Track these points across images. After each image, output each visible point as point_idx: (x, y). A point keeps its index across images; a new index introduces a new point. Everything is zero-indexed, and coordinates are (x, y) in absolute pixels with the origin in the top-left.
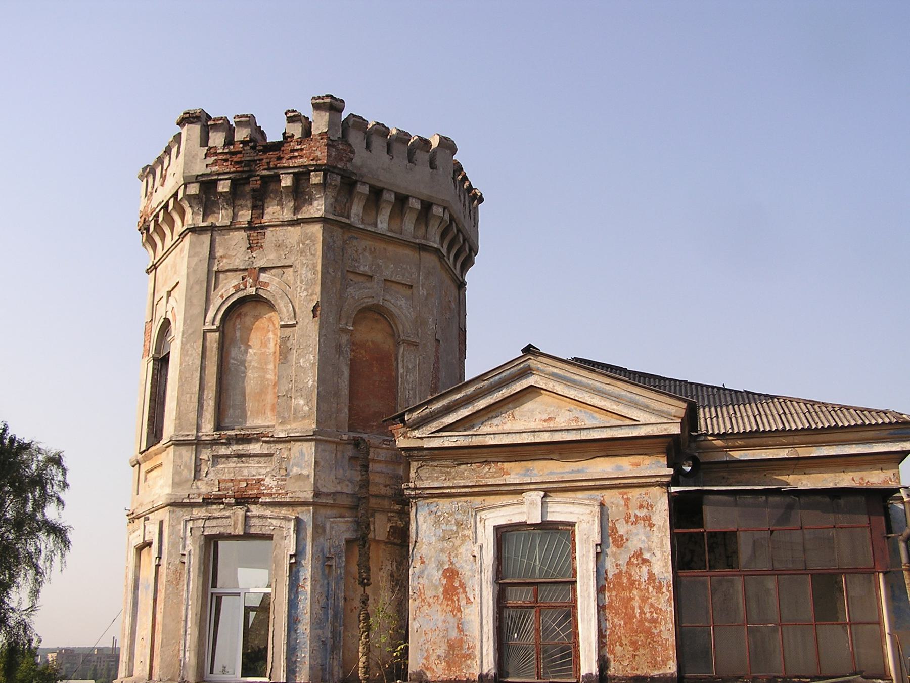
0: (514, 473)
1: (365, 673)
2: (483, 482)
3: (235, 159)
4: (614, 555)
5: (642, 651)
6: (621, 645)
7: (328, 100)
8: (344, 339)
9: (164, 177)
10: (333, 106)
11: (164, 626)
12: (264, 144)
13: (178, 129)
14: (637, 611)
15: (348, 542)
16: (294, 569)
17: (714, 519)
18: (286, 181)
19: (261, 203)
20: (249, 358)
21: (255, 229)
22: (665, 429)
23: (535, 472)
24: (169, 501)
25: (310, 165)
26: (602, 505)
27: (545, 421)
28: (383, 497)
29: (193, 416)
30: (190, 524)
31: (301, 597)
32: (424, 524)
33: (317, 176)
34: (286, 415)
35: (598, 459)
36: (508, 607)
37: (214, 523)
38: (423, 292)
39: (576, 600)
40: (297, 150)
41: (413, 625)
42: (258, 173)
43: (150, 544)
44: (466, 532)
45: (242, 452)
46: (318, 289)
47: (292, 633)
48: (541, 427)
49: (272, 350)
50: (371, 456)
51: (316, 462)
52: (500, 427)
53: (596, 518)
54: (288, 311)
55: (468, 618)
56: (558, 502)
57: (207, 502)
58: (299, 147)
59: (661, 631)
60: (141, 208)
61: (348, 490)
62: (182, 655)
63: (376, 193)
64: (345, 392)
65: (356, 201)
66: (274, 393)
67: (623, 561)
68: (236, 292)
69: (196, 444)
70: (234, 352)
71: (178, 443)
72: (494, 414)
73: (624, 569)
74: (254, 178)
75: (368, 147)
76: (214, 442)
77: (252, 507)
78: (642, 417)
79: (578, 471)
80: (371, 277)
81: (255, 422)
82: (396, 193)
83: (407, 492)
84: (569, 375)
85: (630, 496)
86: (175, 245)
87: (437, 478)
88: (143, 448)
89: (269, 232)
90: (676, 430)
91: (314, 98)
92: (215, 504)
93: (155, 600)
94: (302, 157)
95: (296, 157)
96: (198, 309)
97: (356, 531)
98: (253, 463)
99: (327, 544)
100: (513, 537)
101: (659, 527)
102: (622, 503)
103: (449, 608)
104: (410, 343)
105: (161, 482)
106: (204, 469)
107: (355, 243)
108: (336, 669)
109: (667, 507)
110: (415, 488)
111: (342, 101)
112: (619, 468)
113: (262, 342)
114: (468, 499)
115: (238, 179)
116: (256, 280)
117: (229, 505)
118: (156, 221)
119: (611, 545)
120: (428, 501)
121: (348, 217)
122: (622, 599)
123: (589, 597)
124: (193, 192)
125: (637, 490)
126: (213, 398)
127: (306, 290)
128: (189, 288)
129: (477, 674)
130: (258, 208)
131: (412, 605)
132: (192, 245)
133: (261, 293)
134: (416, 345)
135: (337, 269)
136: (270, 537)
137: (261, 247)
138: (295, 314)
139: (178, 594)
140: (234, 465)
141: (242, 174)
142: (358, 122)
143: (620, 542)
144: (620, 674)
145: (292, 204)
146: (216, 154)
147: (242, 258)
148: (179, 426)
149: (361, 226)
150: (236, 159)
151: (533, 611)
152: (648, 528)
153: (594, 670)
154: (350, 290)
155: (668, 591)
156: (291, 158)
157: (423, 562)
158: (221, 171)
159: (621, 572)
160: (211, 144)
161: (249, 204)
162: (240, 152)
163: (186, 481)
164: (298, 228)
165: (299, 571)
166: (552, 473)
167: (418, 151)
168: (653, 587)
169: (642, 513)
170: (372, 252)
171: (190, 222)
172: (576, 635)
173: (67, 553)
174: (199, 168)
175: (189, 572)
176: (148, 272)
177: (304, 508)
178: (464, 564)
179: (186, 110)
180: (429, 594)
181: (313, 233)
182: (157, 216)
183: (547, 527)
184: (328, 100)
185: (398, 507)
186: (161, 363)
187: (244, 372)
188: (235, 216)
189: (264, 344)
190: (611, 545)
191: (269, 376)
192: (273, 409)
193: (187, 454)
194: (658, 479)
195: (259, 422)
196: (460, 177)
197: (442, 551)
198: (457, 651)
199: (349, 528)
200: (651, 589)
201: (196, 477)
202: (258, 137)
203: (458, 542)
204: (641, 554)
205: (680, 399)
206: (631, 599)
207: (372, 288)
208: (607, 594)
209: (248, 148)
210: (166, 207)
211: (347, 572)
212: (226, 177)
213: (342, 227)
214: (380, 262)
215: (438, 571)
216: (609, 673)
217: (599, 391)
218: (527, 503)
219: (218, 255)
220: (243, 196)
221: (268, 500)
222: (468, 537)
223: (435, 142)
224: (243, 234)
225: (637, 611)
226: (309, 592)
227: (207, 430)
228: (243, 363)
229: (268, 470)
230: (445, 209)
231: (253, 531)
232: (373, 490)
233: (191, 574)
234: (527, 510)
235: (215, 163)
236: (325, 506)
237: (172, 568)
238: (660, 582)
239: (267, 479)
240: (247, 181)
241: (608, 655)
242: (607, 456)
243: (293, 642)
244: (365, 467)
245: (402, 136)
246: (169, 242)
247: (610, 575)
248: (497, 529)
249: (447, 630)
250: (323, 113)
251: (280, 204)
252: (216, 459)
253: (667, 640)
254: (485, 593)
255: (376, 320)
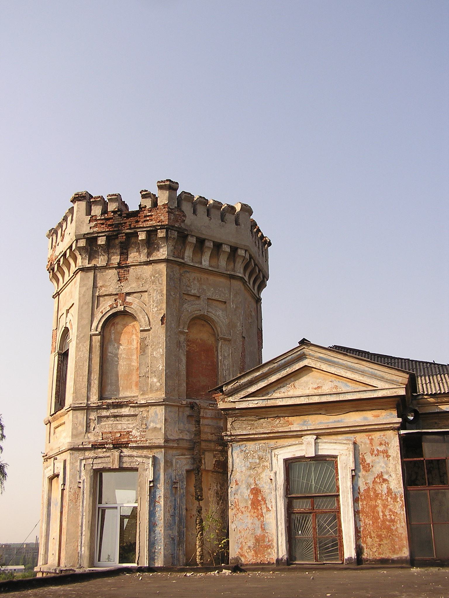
0: (296, 424)
1: (201, 559)
2: (276, 430)
3: (109, 223)
4: (364, 477)
5: (385, 541)
6: (371, 537)
7: (168, 183)
8: (182, 338)
9: (63, 236)
10: (170, 186)
11: (68, 530)
12: (127, 212)
13: (72, 205)
14: (381, 514)
15: (188, 471)
16: (152, 491)
17: (430, 451)
18: (142, 236)
19: (126, 251)
20: (120, 352)
21: (122, 268)
22: (395, 392)
23: (310, 422)
24: (70, 447)
25: (157, 225)
26: (355, 443)
27: (315, 389)
28: (210, 441)
29: (85, 391)
30: (84, 462)
31: (158, 509)
32: (238, 459)
33: (162, 232)
34: (145, 389)
35: (351, 413)
36: (294, 513)
37: (99, 461)
38: (233, 306)
39: (339, 508)
40: (148, 216)
41: (232, 527)
42: (123, 231)
43: (57, 476)
44: (266, 464)
45: (117, 414)
46: (164, 306)
47: (152, 533)
48: (313, 393)
49: (135, 347)
50: (202, 414)
51: (165, 419)
52: (286, 394)
53: (351, 453)
54: (145, 321)
55: (268, 520)
56: (325, 442)
57: (95, 447)
58: (150, 214)
59: (397, 528)
60: (49, 256)
61: (187, 437)
62: (79, 550)
63: (201, 242)
64: (184, 372)
65: (188, 248)
66: (137, 374)
67: (370, 481)
68: (111, 309)
69: (87, 409)
70: (110, 349)
71: (75, 409)
72: (281, 385)
73: (371, 486)
74: (121, 235)
75: (195, 212)
76: (99, 408)
77: (124, 450)
78: (380, 384)
79: (338, 421)
80: (199, 297)
81: (125, 394)
82: (213, 242)
83: (225, 438)
84: (330, 358)
85: (373, 437)
86: (71, 280)
87: (245, 428)
88: (53, 412)
89: (131, 269)
90: (402, 392)
91: (159, 182)
92: (100, 448)
93: (61, 513)
94: (152, 220)
95: (148, 220)
96: (87, 321)
97: (193, 464)
98: (124, 421)
99: (174, 474)
100: (296, 467)
101: (394, 457)
102: (368, 442)
103: (255, 515)
104: (225, 340)
105: (64, 434)
106: (92, 425)
107: (188, 275)
108: (181, 557)
109: (398, 444)
110: (231, 435)
111: (177, 183)
112: (365, 419)
113: (128, 341)
114: (266, 441)
115: (111, 236)
116: (124, 301)
117: (109, 449)
118: (59, 264)
119: (362, 470)
120: (240, 443)
121: (183, 259)
122: (370, 506)
123: (348, 505)
124: (82, 245)
125: (378, 433)
126: (97, 379)
127: (156, 307)
128: (80, 307)
129: (275, 558)
130: (124, 254)
131: (231, 513)
132: (82, 279)
133: (127, 309)
134: (229, 340)
135: (177, 294)
136: (136, 470)
137: (127, 279)
138: (149, 322)
139: (76, 509)
140: (111, 423)
141: (113, 232)
142: (188, 196)
143: (368, 468)
144: (371, 557)
145: (146, 251)
146: (96, 220)
147: (114, 287)
148: (75, 398)
150: (109, 223)
151: (311, 515)
152: (386, 459)
153: (353, 555)
154: (185, 306)
155: (401, 500)
156: (145, 221)
157: (237, 484)
158: (100, 231)
159: (369, 488)
160: (93, 213)
161: (118, 252)
162: (112, 218)
163: (81, 433)
164: (151, 266)
165: (155, 492)
166: (321, 423)
167: (227, 214)
168: (391, 498)
169: (381, 448)
171: (80, 264)
172: (340, 531)
173: (5, 482)
174: (86, 229)
175: (83, 494)
176: (54, 297)
177: (158, 450)
178: (264, 485)
179: (76, 192)
180: (242, 505)
181: (160, 270)
182: (59, 261)
183: (318, 459)
184: (168, 183)
185: (220, 448)
186: (63, 356)
187: (118, 362)
188: (109, 260)
189: (130, 342)
190: (362, 470)
191: (133, 364)
192: (137, 385)
193: (81, 416)
194: (392, 425)
195: (128, 394)
196: (255, 230)
197: (250, 476)
198: (261, 543)
199: (188, 463)
200: (389, 499)
201: (87, 431)
202: (123, 208)
203: (260, 470)
204: (382, 475)
205: (404, 372)
206: (376, 506)
207: (200, 304)
208: (360, 503)
209: (117, 215)
210: (65, 255)
211: (187, 492)
212: (103, 234)
213: (179, 265)
215: (247, 489)
216: (363, 556)
217: (350, 368)
218: (305, 443)
219: (99, 285)
220: (114, 247)
221: (134, 445)
222: (267, 466)
223: (238, 208)
224: (115, 271)
225: (381, 514)
226: (163, 506)
227: (94, 400)
228: (116, 355)
229: (134, 425)
230: (246, 251)
231: (125, 465)
232: (203, 437)
233: (85, 495)
234: (305, 448)
235: (96, 226)
236: (172, 448)
237: (73, 491)
238: (395, 495)
239: (134, 431)
240: (116, 237)
241: (362, 545)
242: (357, 411)
243: (152, 539)
244: (198, 422)
245: (217, 204)
246: (67, 278)
247: (362, 490)
248: (286, 461)
249: (254, 529)
250: (165, 191)
251: (139, 251)
252: (100, 418)
253: (401, 534)
254: (279, 504)
255: (203, 325)
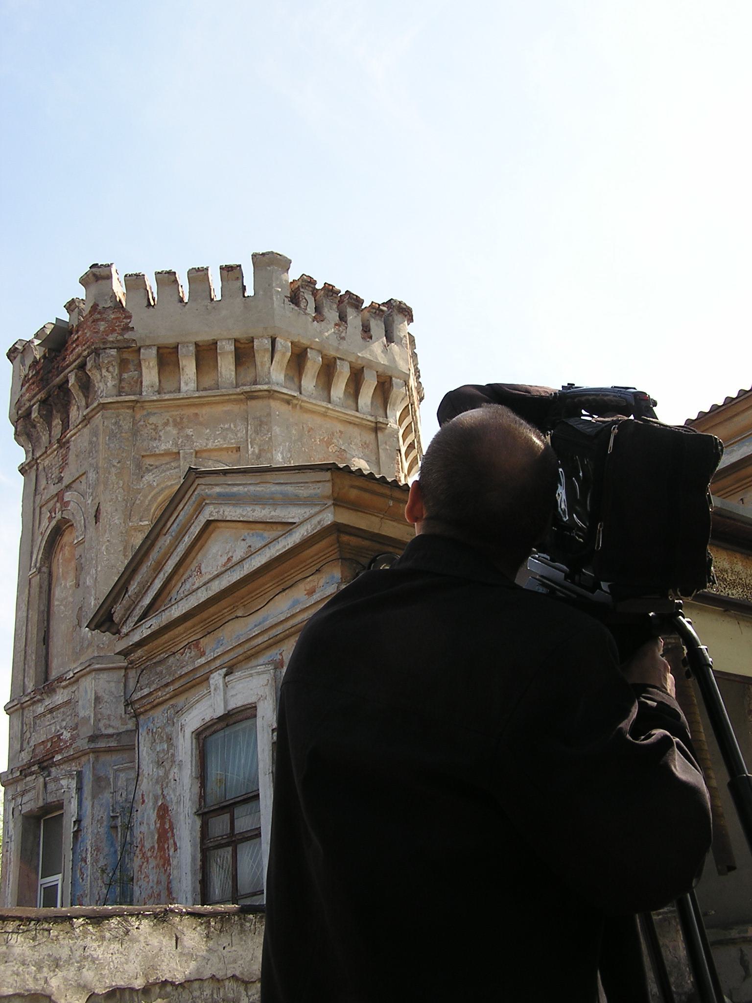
22: (319, 522)
68: (50, 522)
78: (293, 514)
107: (152, 420)
149: (155, 398)
170: (176, 424)
214: (189, 432)
236: (109, 750)
